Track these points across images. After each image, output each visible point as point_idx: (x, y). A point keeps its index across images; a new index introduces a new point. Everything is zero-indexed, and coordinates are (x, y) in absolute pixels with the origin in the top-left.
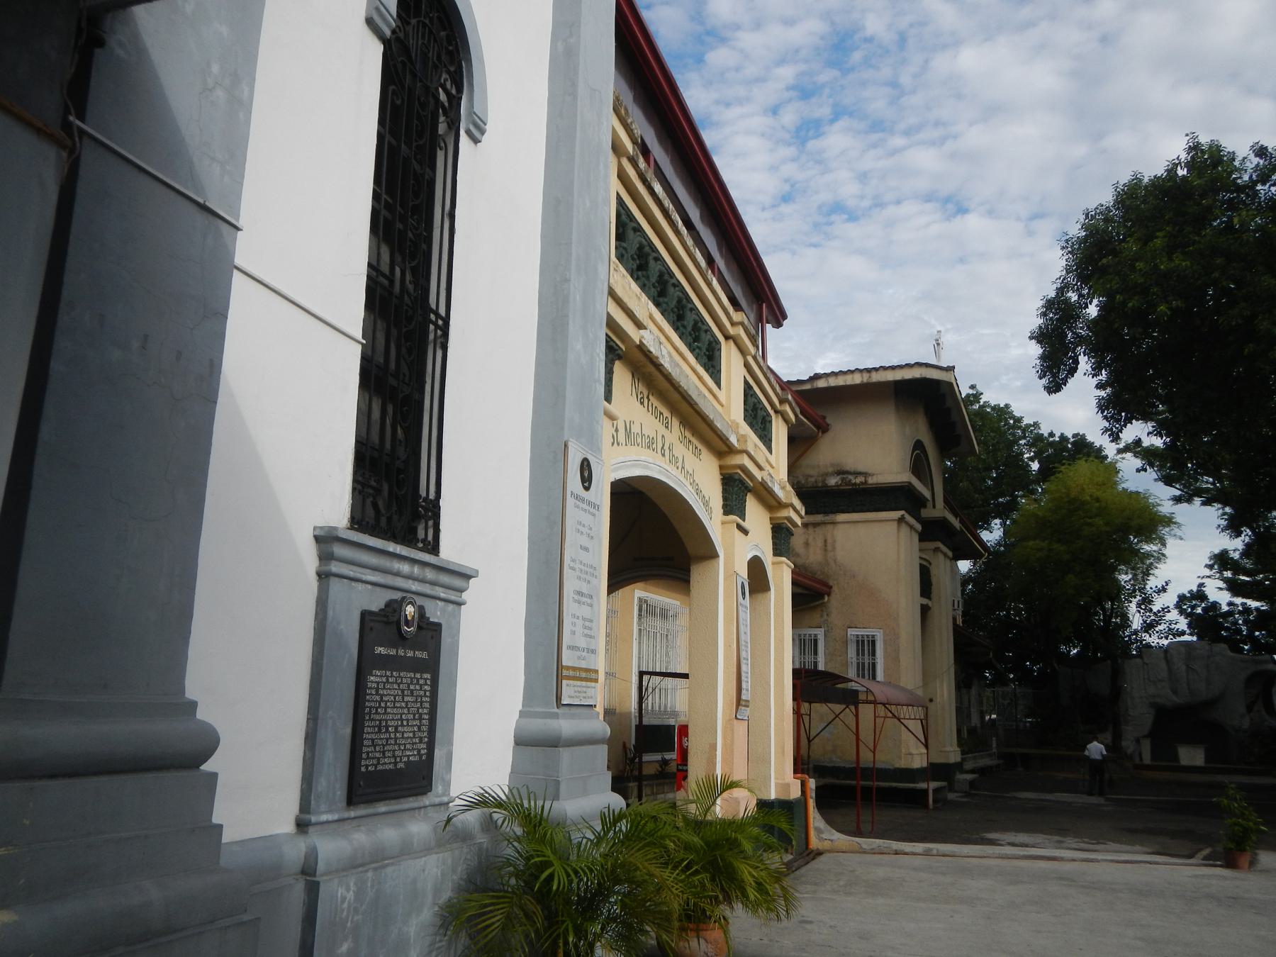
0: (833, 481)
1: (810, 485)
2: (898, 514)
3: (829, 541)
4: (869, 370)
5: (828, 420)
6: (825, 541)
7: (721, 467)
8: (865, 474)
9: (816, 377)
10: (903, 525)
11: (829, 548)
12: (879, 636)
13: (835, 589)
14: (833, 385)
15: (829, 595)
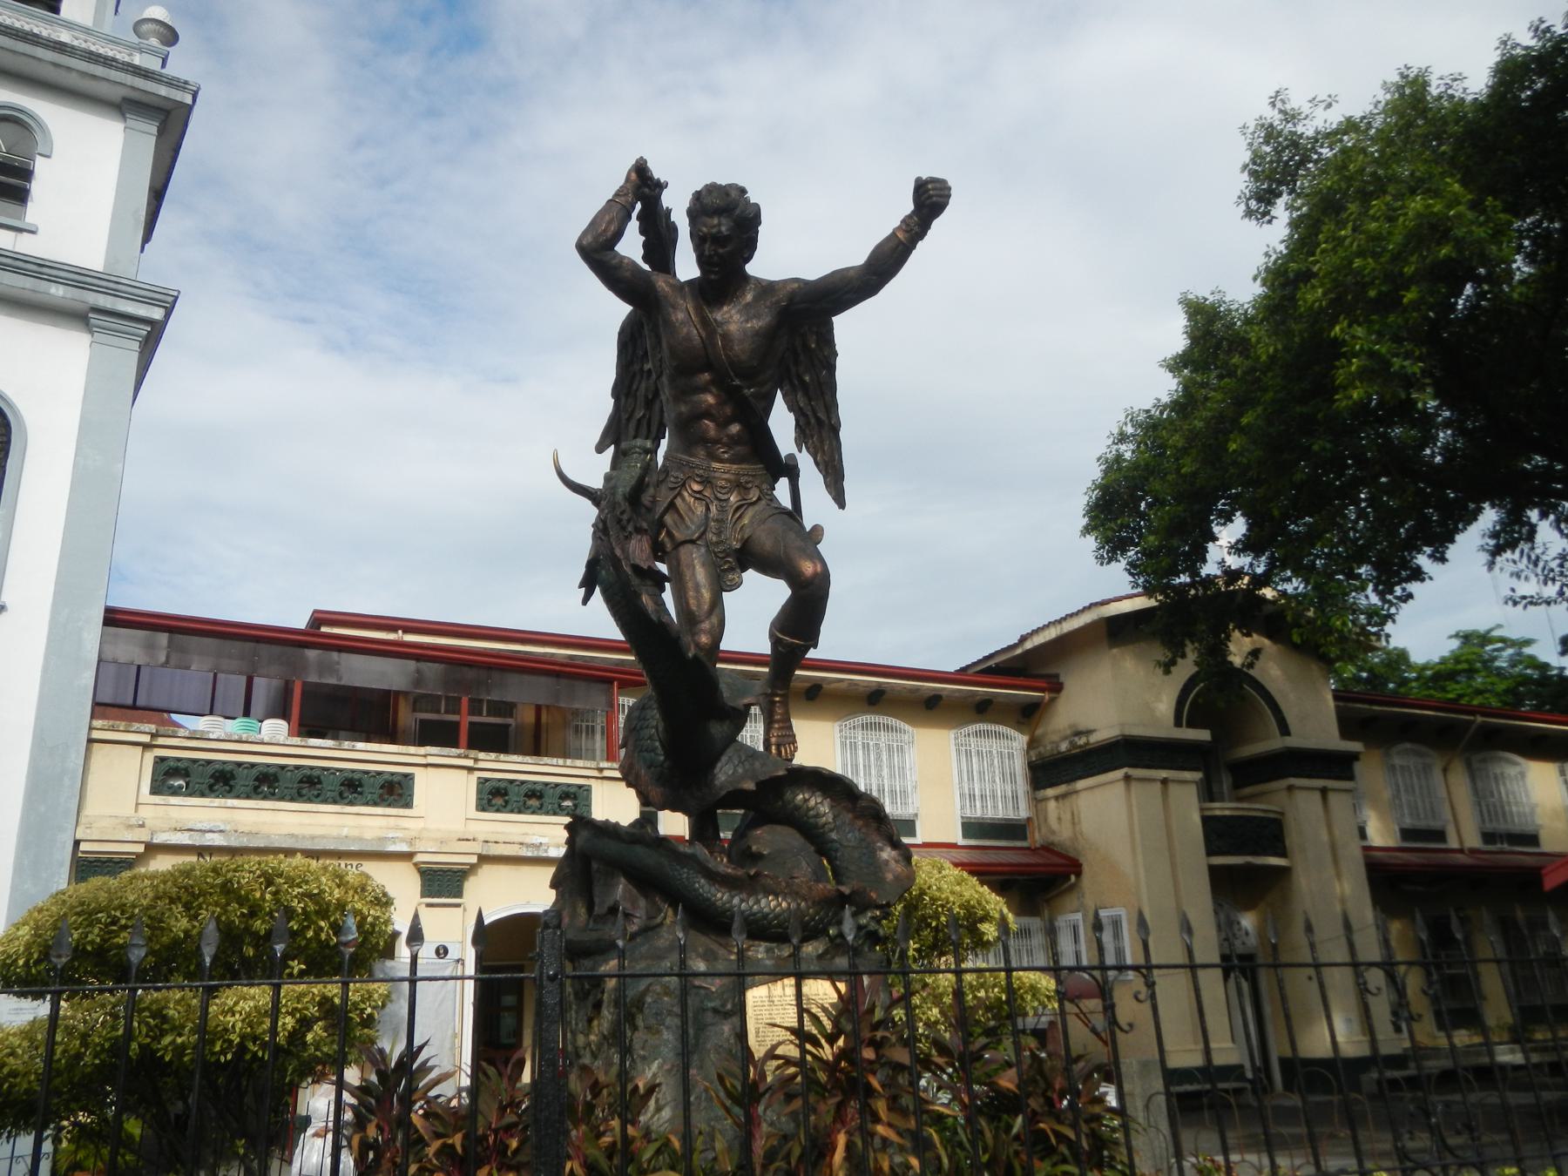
0: (1064, 747)
1: (1048, 754)
2: (1119, 774)
3: (1076, 813)
4: (1060, 621)
5: (1062, 679)
6: (1073, 814)
7: (415, 864)
8: (1089, 732)
9: (1023, 639)
10: (1134, 785)
11: (1076, 820)
12: (1121, 912)
13: (1086, 869)
14: (1036, 644)
15: (1079, 874)
